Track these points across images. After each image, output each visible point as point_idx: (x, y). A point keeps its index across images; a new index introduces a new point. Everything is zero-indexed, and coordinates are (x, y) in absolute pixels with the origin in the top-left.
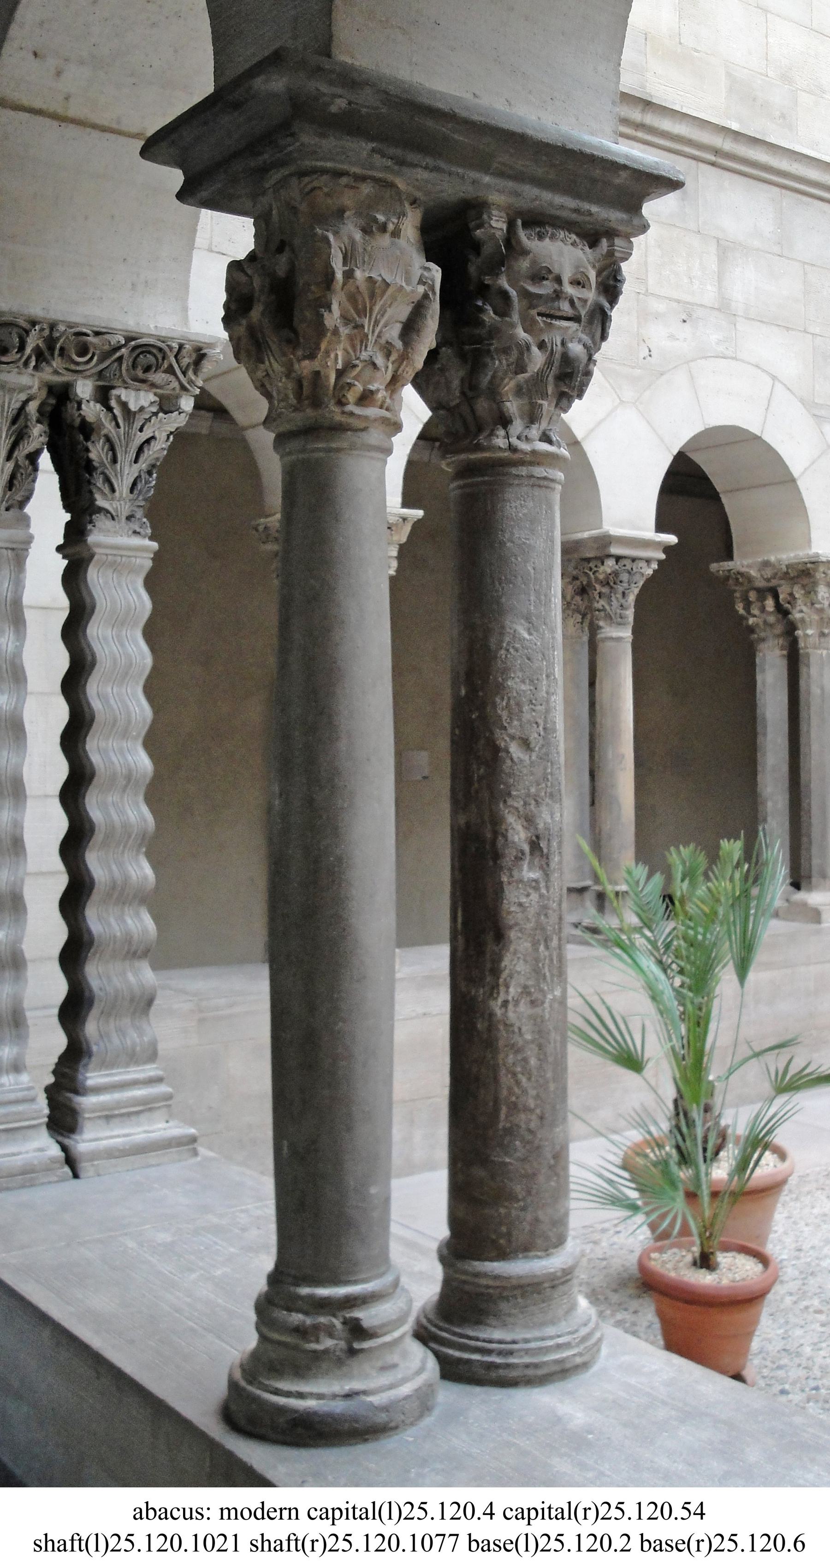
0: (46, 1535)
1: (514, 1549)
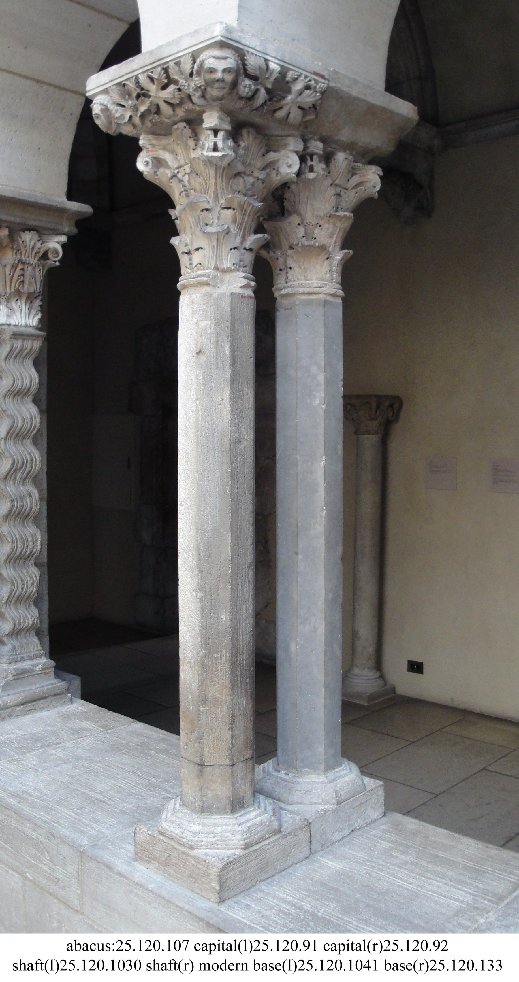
1: (413, 969)
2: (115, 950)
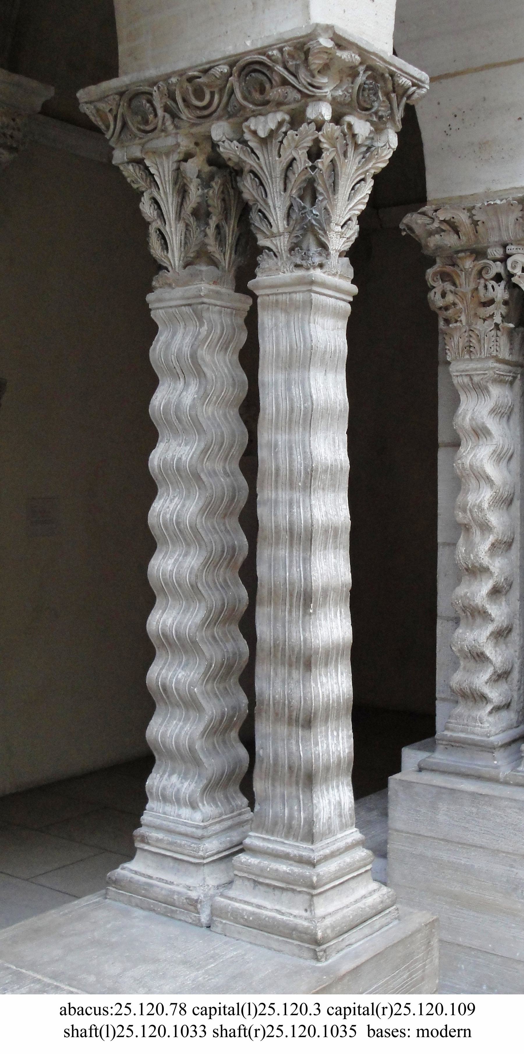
0: (73, 1026)
2: (114, 1014)
